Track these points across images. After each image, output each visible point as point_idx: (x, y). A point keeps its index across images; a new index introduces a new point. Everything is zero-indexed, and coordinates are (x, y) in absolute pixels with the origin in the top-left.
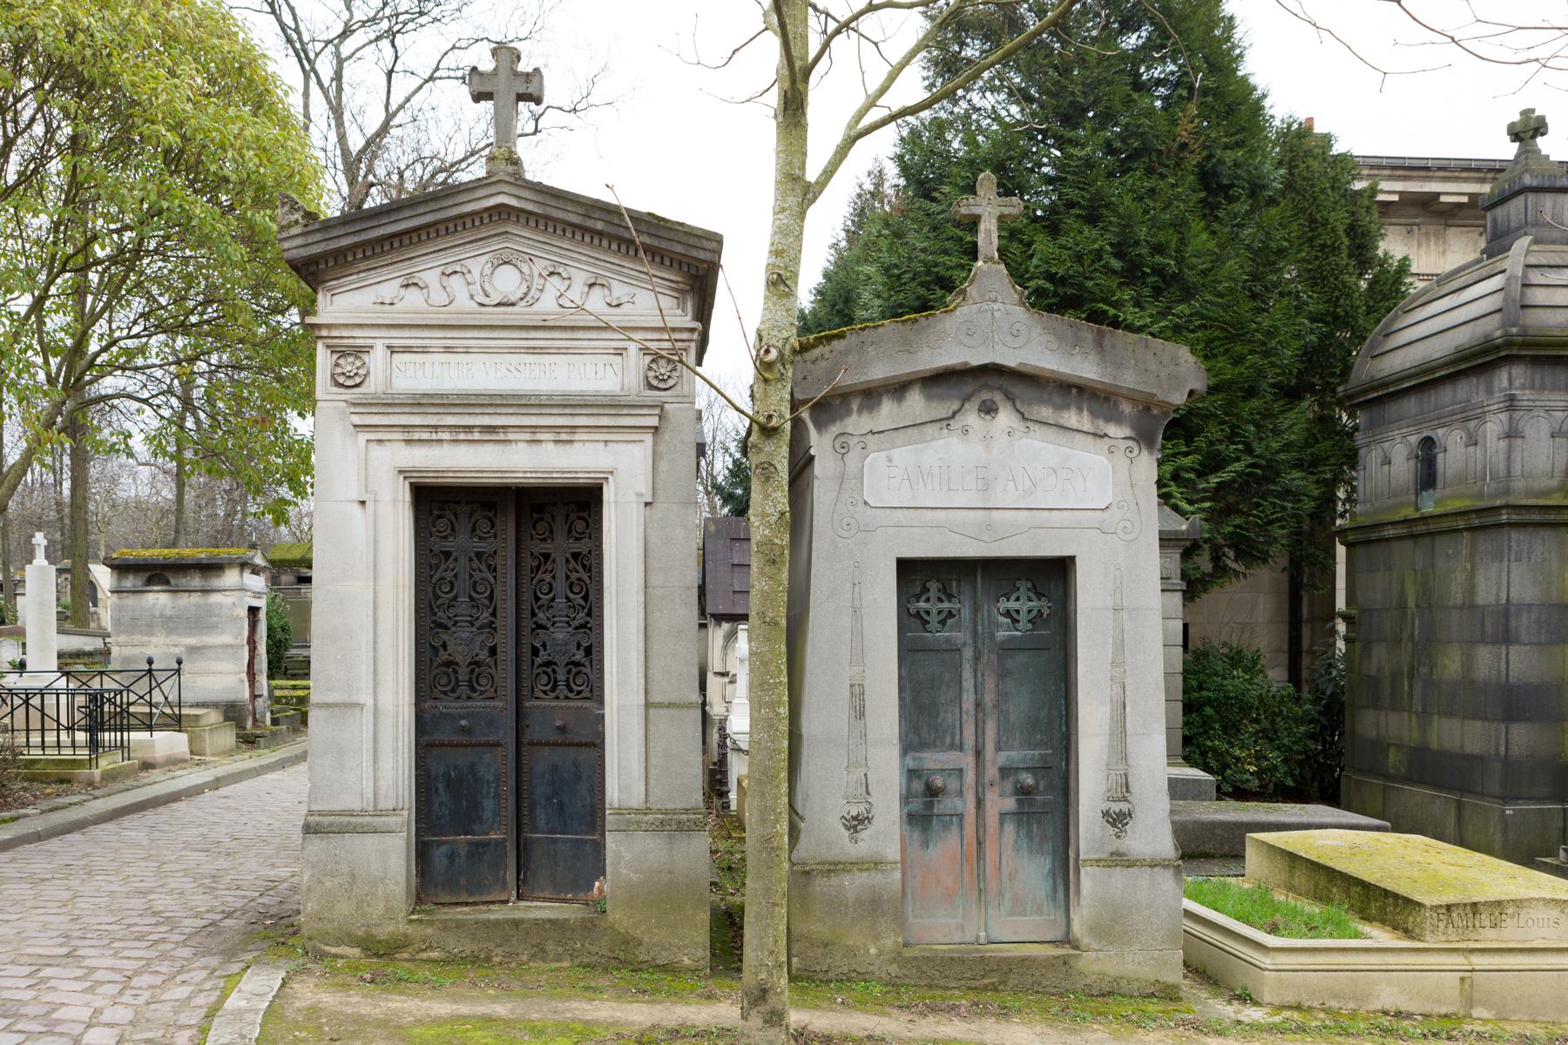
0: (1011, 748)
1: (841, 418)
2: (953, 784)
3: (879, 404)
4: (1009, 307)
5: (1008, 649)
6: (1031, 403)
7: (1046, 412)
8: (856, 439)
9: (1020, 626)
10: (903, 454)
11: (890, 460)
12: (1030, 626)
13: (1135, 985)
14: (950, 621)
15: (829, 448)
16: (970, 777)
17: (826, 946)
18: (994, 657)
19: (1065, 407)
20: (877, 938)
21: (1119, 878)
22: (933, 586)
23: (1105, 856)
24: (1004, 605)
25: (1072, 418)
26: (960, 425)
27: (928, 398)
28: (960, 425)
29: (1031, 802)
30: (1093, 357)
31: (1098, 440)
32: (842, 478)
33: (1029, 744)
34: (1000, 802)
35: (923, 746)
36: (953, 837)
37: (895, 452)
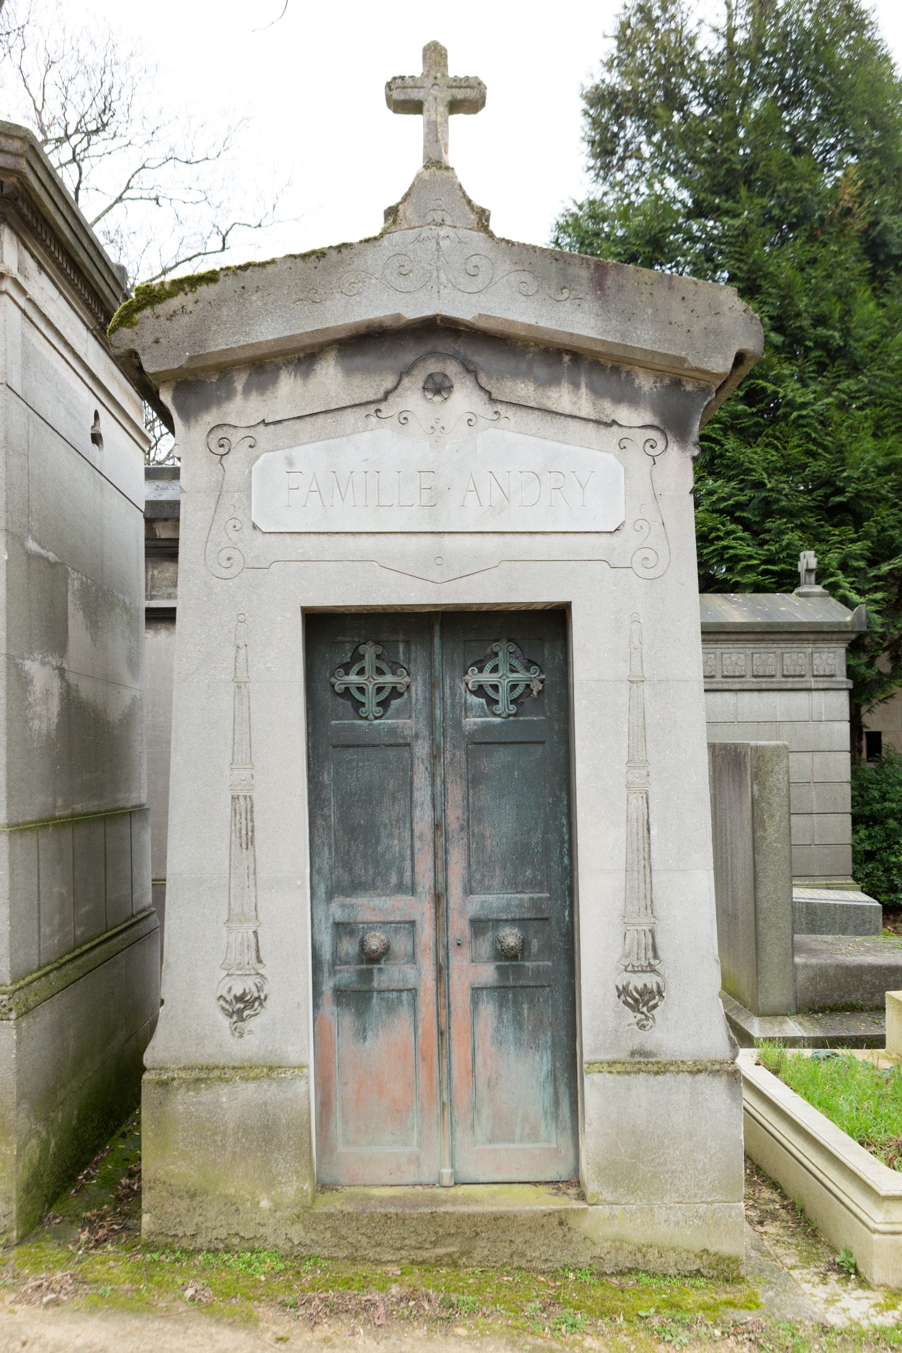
0: (488, 890)
1: (219, 402)
2: (400, 944)
3: (275, 380)
4: (463, 233)
5: (482, 742)
6: (501, 377)
7: (524, 390)
8: (242, 433)
9: (500, 708)
10: (311, 454)
11: (290, 463)
12: (513, 709)
13: (672, 1257)
14: (395, 703)
15: (201, 447)
16: (426, 933)
17: (193, 1196)
18: (460, 755)
19: (553, 381)
20: (271, 1183)
21: (642, 1088)
22: (369, 652)
23: (623, 1056)
24: (474, 677)
25: (563, 398)
26: (395, 411)
27: (348, 372)
28: (395, 411)
29: (519, 971)
30: (590, 304)
31: (603, 430)
32: (220, 492)
33: (514, 885)
34: (473, 970)
35: (356, 887)
36: (402, 1024)
37: (298, 452)
